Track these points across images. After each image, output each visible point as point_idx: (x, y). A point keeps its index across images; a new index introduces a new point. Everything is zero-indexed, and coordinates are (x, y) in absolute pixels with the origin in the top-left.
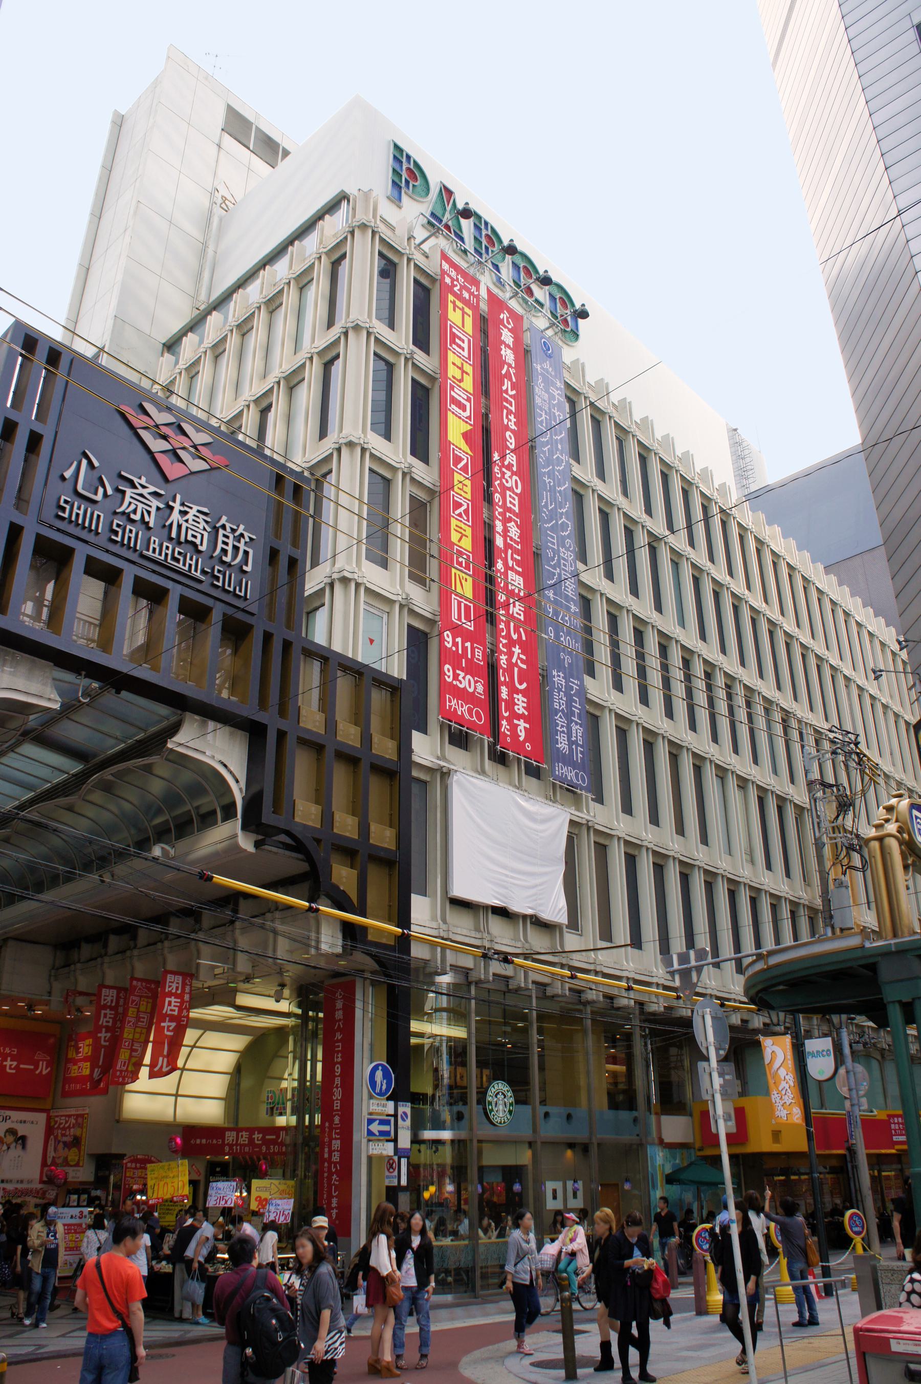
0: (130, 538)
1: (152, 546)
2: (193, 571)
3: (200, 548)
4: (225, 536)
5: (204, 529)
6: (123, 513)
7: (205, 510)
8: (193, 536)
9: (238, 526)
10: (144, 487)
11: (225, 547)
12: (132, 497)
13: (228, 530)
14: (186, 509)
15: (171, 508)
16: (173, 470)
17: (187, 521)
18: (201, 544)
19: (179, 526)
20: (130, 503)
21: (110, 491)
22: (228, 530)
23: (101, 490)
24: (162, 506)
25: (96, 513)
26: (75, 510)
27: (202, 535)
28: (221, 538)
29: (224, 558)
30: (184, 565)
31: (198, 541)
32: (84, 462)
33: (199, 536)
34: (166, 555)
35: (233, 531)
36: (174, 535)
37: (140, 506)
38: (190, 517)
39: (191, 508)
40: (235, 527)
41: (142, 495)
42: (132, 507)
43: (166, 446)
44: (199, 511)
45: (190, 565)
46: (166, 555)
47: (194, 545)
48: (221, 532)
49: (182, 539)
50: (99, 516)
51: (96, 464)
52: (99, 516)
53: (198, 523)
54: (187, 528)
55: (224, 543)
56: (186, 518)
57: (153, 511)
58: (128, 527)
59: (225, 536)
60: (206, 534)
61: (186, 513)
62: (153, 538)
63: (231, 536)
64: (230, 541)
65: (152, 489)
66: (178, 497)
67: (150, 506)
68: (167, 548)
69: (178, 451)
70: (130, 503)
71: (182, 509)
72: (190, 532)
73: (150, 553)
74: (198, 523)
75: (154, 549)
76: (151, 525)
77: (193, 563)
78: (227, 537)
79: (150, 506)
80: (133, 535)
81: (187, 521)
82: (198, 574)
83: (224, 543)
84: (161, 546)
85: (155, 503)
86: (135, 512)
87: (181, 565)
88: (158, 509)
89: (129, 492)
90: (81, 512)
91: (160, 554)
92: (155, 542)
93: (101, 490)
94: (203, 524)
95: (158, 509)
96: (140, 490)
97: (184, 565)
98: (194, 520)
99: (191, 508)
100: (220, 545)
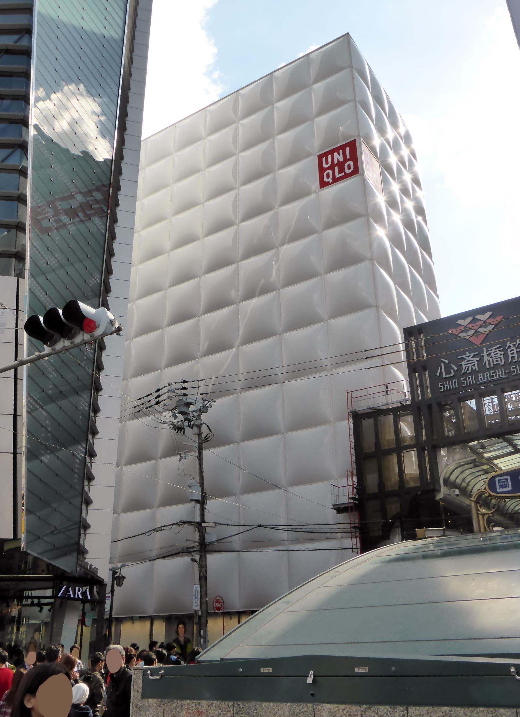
0: (470, 381)
1: (480, 378)
2: (501, 377)
3: (501, 364)
4: (511, 351)
5: (501, 354)
6: (464, 373)
7: (499, 346)
8: (496, 361)
9: (516, 342)
10: (468, 357)
11: (513, 355)
12: (465, 365)
13: (512, 346)
14: (490, 352)
15: (483, 356)
16: (477, 341)
17: (492, 357)
18: (501, 362)
19: (489, 361)
20: (465, 367)
21: (456, 369)
22: (512, 346)
23: (452, 371)
24: (478, 359)
25: (453, 381)
26: (445, 386)
27: (500, 358)
28: (509, 352)
29: (514, 361)
30: (496, 376)
31: (499, 362)
32: (443, 365)
33: (499, 359)
34: (487, 377)
35: (514, 345)
36: (488, 367)
37: (470, 365)
38: (492, 354)
39: (492, 350)
40: (515, 343)
41: (469, 361)
42: (467, 368)
43: (471, 332)
44: (496, 349)
45: (499, 375)
46: (487, 377)
47: (499, 364)
48: (509, 350)
49: (492, 366)
50: (455, 381)
51: (447, 361)
52: (455, 381)
53: (497, 354)
54: (493, 360)
55: (512, 354)
56: (491, 356)
57: (476, 364)
58: (468, 377)
59: (511, 351)
60: (502, 356)
61: (490, 353)
62: (479, 375)
63: (514, 349)
64: (515, 351)
65: (472, 355)
66: (485, 349)
67: (474, 362)
68: (487, 374)
69: (478, 330)
70: (465, 367)
71: (488, 353)
72: (494, 361)
73: (480, 381)
74: (497, 354)
75: (481, 379)
76: (477, 369)
77: (500, 373)
78: (513, 350)
79: (474, 362)
80: (471, 380)
81: (492, 357)
82: (504, 376)
83: (513, 353)
84: (483, 376)
85: (475, 360)
86: (468, 369)
87: (495, 378)
88: (477, 361)
89: (463, 363)
90: (448, 385)
91: (484, 379)
92: (480, 375)
93: (452, 371)
94: (499, 353)
95: (477, 361)
96: (468, 359)
97: (496, 376)
98: (495, 354)
99: (492, 350)
100: (510, 356)
